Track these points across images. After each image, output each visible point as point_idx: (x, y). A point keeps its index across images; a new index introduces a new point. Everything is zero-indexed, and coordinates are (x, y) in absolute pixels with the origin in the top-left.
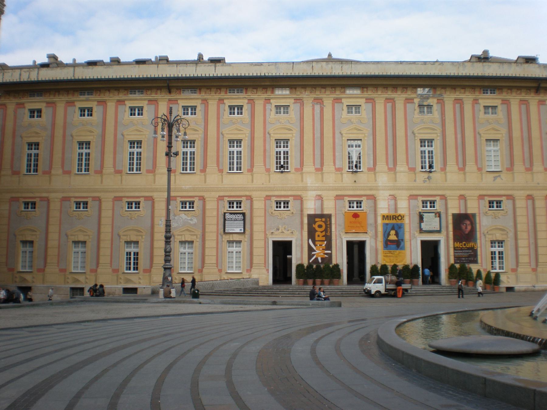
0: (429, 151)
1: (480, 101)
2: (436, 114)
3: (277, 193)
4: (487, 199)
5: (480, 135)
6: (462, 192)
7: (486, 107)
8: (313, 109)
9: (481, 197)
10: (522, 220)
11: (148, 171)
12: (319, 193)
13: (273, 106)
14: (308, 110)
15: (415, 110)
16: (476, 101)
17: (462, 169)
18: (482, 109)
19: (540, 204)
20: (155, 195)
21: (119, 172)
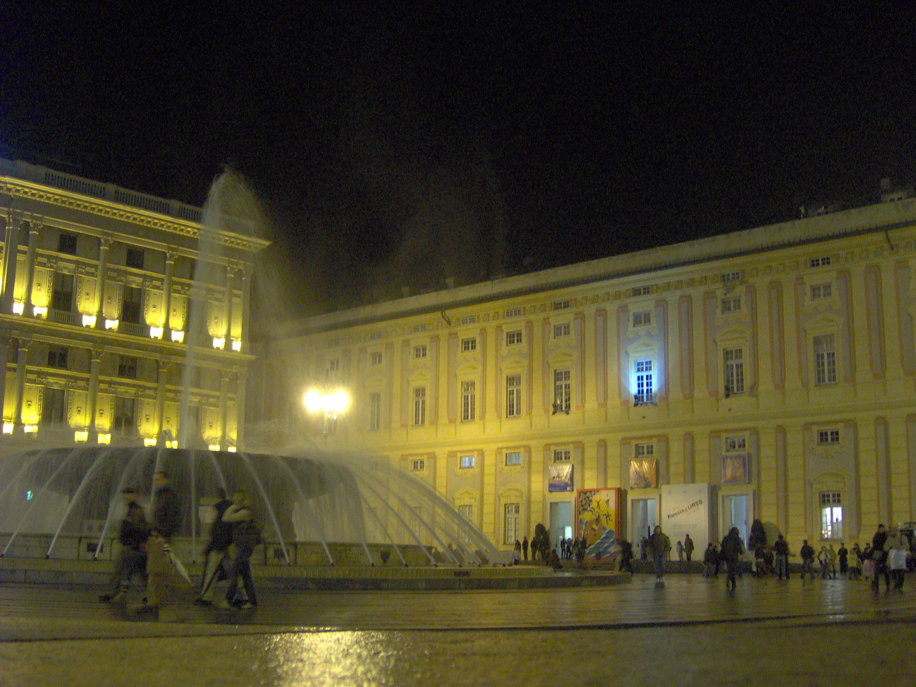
0: (737, 366)
1: (806, 279)
2: (745, 309)
3: (555, 440)
4: (816, 429)
5: (805, 331)
6: (780, 421)
7: (815, 290)
8: (596, 324)
9: (808, 426)
10: (868, 457)
11: (431, 423)
12: (602, 436)
13: (552, 327)
14: (590, 326)
15: (717, 307)
16: (800, 280)
17: (780, 385)
18: (808, 291)
19: (897, 430)
20: (438, 451)
21: (404, 426)
